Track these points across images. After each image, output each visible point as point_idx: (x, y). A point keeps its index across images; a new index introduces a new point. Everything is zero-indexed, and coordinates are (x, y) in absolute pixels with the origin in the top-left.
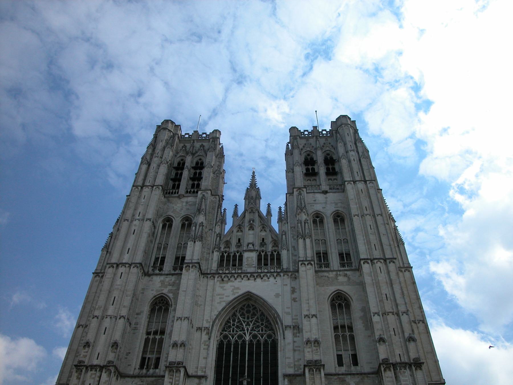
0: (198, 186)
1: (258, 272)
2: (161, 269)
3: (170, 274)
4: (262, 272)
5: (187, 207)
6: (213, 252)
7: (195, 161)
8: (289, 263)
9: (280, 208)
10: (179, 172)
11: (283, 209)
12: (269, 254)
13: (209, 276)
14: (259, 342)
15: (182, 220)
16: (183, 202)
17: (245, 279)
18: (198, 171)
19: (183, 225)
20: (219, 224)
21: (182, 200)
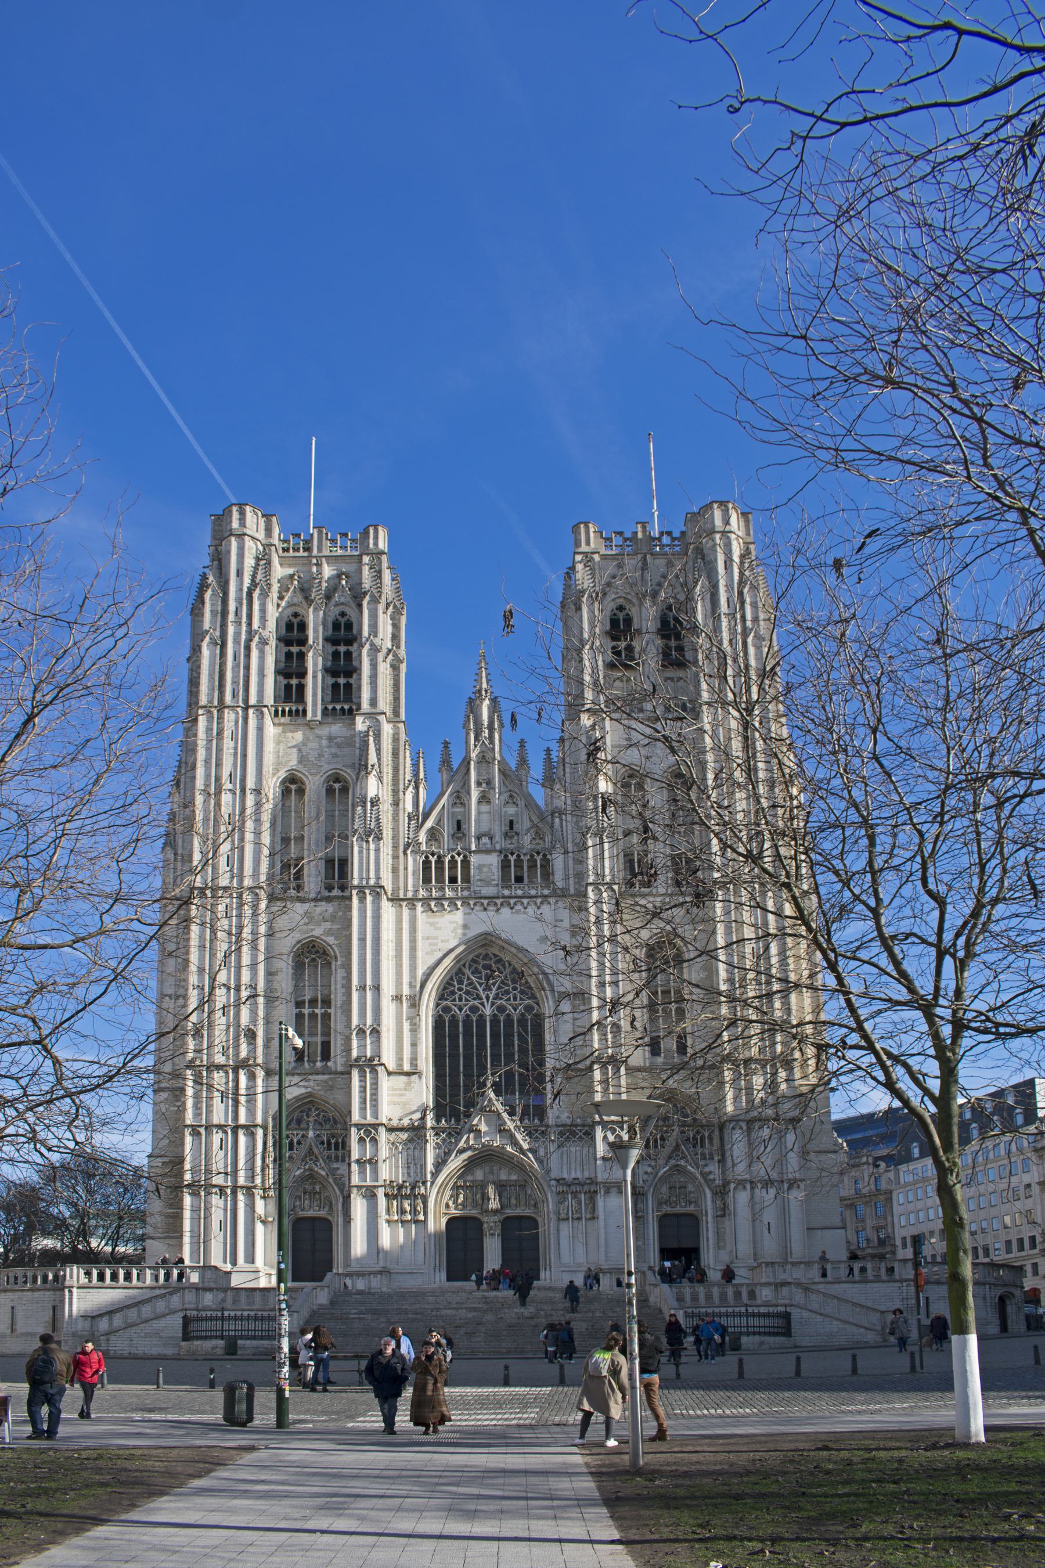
0: (348, 686)
1: (504, 897)
2: (299, 888)
3: (321, 900)
4: (510, 897)
5: (334, 750)
6: (405, 853)
7: (330, 620)
8: (567, 878)
9: (548, 751)
10: (295, 649)
11: (554, 755)
12: (525, 859)
13: (404, 904)
14: (509, 1019)
15: (327, 780)
16: (320, 737)
17: (477, 908)
18: (342, 649)
19: (330, 791)
20: (411, 789)
21: (317, 731)
